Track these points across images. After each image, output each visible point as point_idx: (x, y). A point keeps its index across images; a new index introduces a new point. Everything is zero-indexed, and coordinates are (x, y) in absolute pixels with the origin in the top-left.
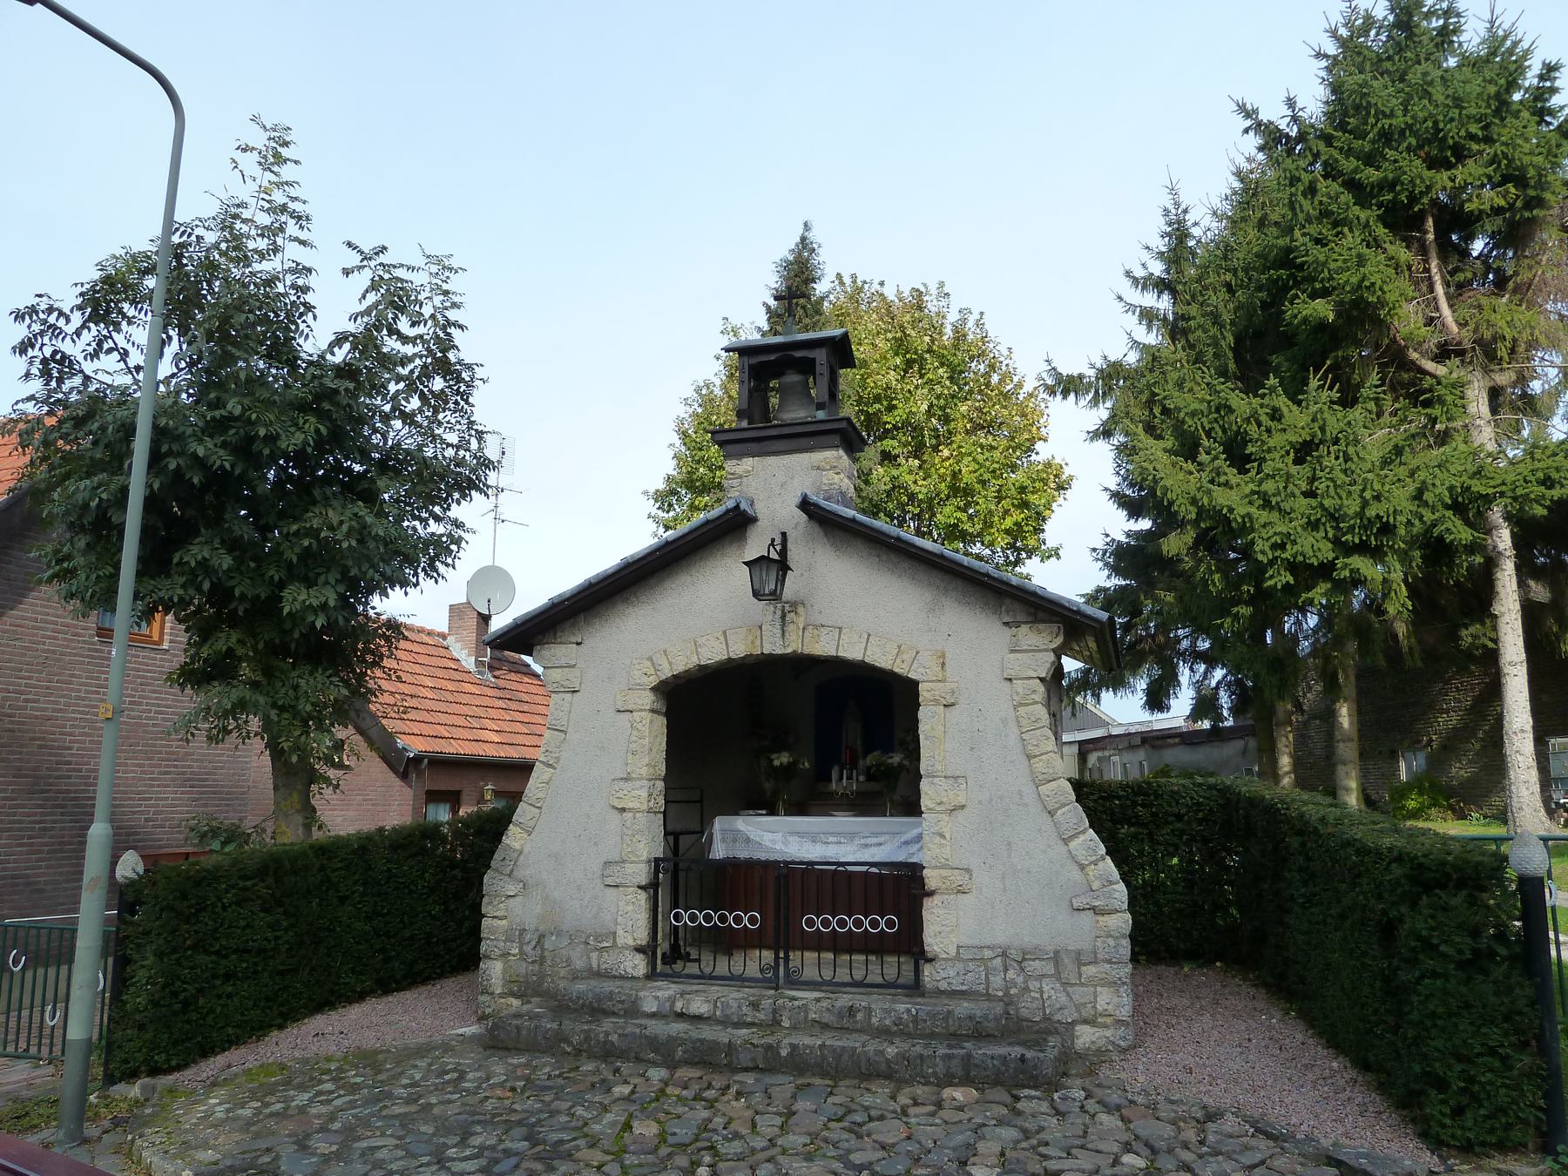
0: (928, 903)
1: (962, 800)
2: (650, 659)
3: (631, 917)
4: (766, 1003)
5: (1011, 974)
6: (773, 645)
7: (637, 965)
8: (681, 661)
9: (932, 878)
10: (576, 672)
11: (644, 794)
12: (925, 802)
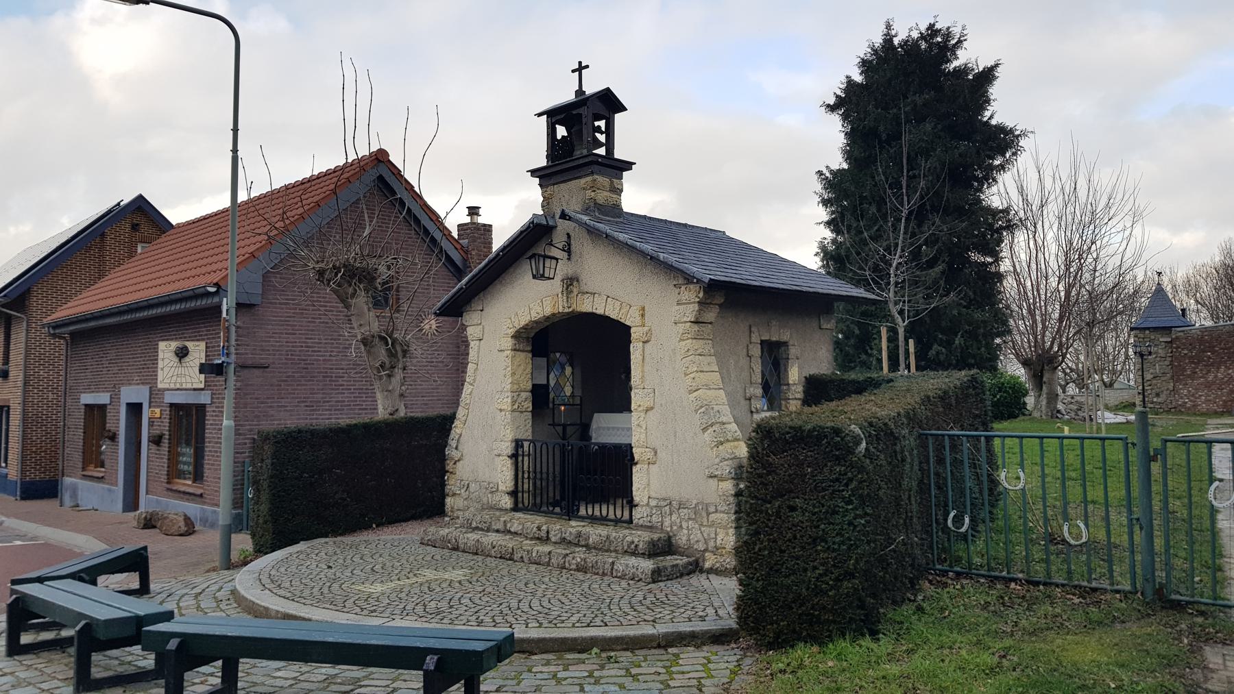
5: (674, 517)
6: (561, 307)
7: (507, 502)
11: (509, 400)
12: (633, 406)
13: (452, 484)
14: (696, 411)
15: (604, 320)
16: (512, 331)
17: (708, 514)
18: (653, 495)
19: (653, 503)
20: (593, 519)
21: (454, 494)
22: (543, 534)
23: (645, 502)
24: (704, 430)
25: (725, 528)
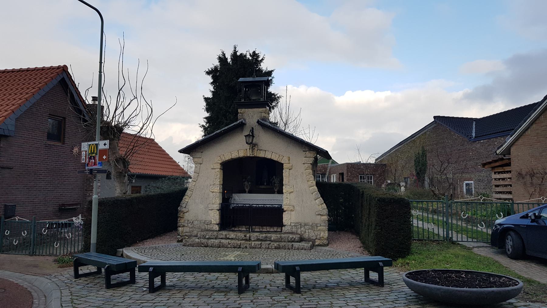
0: (284, 213)
1: (292, 190)
3: (215, 217)
4: (248, 235)
5: (302, 229)
6: (249, 154)
7: (217, 228)
8: (227, 157)
9: (285, 207)
10: (201, 159)
12: (284, 191)
13: (181, 222)
14: (312, 194)
15: (271, 161)
16: (220, 162)
17: (317, 227)
18: (292, 221)
19: (292, 224)
20: (261, 232)
21: (184, 226)
22: (248, 238)
23: (289, 224)
24: (315, 200)
25: (324, 231)
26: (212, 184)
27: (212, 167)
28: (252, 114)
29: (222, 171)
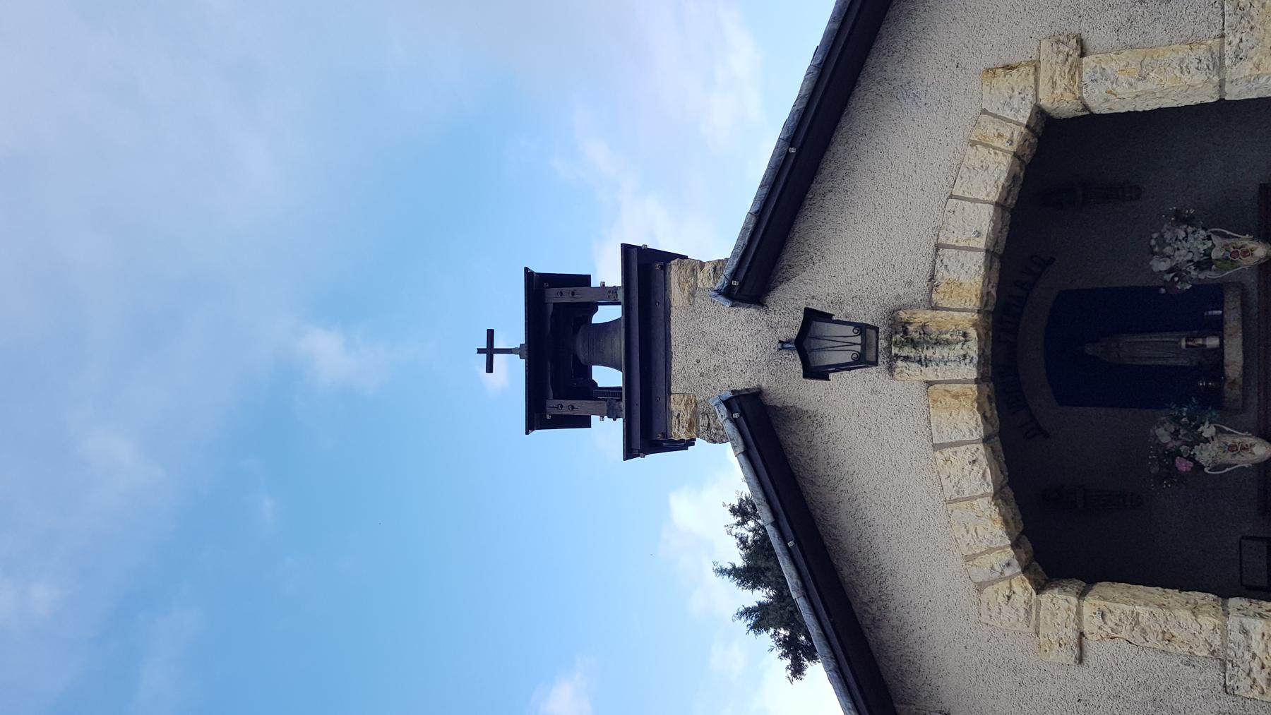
2: (980, 587)
6: (960, 368)
16: (1022, 588)
26: (1213, 674)
27: (1069, 656)
28: (700, 352)
29: (1104, 588)
